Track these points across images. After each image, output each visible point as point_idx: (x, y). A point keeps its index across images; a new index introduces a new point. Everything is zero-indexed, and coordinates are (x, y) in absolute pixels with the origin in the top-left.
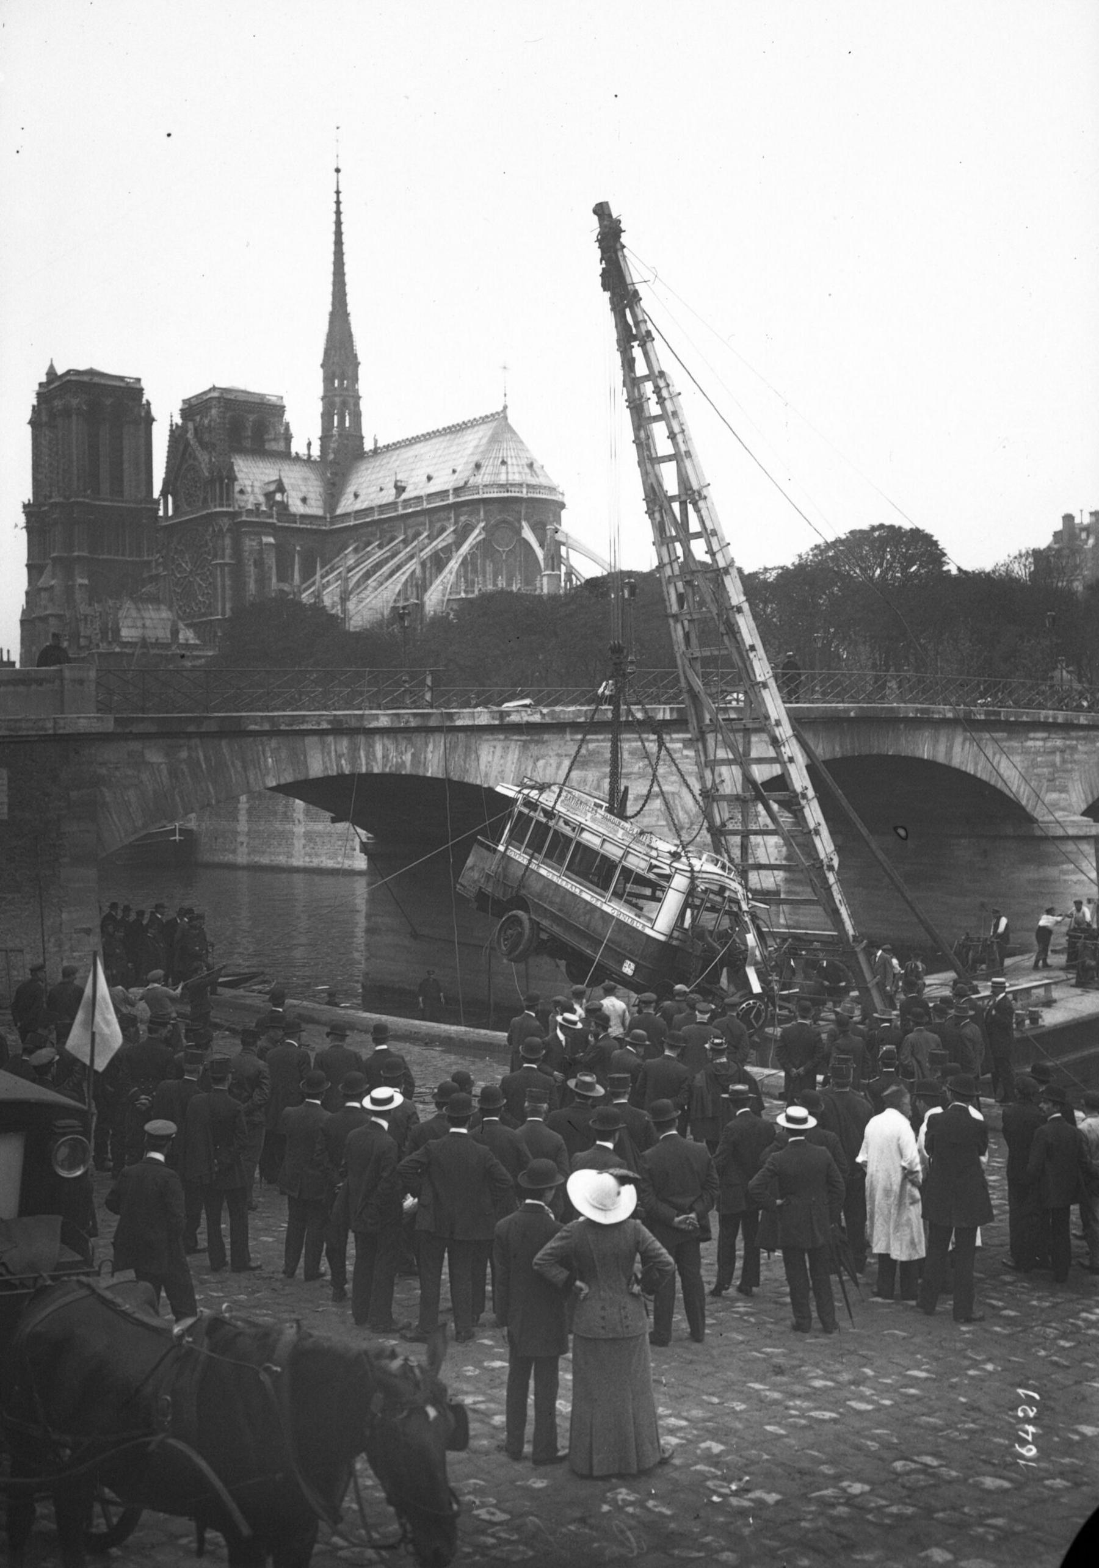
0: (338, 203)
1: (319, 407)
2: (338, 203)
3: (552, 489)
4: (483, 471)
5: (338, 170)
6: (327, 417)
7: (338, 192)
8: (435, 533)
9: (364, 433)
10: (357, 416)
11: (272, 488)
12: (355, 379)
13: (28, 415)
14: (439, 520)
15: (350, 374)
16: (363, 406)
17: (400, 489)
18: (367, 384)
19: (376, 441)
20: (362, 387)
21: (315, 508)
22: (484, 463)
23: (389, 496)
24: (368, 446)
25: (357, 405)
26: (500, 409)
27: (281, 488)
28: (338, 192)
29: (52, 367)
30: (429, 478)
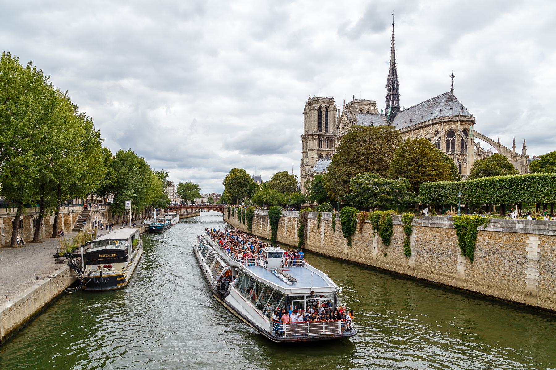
0: (393, 34)
1: (385, 99)
2: (393, 34)
3: (472, 117)
4: (443, 112)
5: (393, 24)
6: (388, 101)
8: (424, 135)
9: (400, 106)
10: (398, 101)
11: (369, 124)
12: (398, 89)
13: (303, 112)
14: (426, 130)
15: (396, 88)
16: (400, 98)
18: (402, 91)
20: (400, 92)
22: (443, 110)
23: (408, 124)
24: (401, 109)
25: (398, 97)
26: (450, 90)
28: (393, 31)
30: (422, 117)
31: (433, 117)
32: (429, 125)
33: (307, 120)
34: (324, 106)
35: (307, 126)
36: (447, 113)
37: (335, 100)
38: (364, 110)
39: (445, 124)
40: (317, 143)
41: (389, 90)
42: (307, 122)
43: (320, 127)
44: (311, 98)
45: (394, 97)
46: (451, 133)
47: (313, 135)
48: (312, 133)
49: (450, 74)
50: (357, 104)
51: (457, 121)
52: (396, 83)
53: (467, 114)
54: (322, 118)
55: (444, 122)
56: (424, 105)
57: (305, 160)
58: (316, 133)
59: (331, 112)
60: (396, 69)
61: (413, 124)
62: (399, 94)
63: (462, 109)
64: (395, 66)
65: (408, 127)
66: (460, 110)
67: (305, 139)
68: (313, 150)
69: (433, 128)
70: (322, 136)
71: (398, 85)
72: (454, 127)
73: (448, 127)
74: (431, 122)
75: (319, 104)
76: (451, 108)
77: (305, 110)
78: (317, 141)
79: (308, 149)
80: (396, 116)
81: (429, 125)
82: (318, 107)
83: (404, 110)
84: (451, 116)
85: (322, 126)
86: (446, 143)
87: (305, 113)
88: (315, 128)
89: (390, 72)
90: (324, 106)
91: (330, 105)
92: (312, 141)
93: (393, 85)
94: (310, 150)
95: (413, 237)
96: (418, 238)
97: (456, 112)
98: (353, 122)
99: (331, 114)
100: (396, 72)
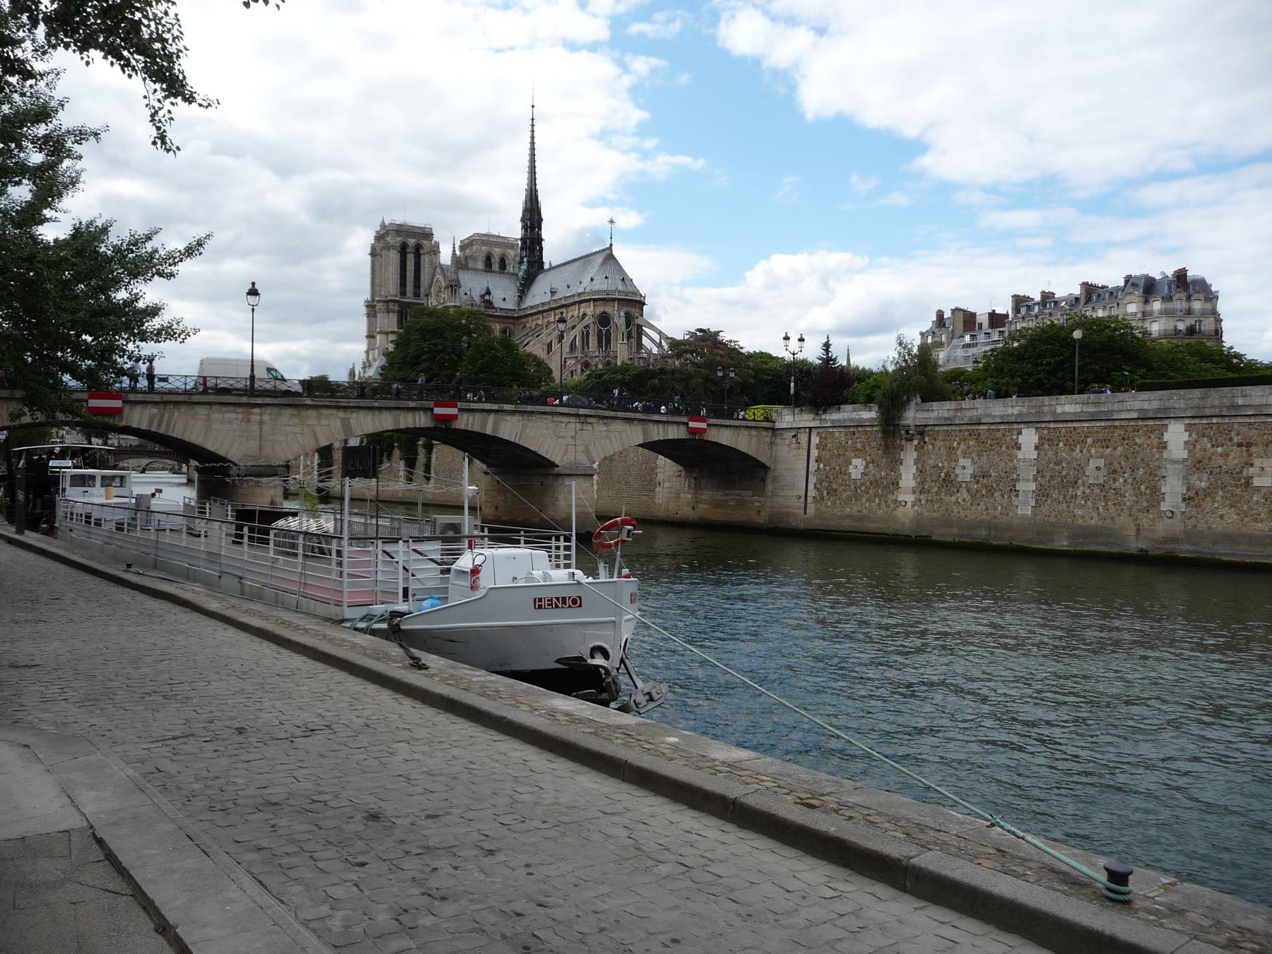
3: (636, 293)
5: (533, 107)
7: (533, 119)
12: (540, 229)
13: (369, 250)
14: (571, 311)
17: (553, 293)
19: (550, 264)
20: (545, 233)
21: (510, 304)
22: (595, 278)
23: (547, 298)
24: (546, 266)
26: (608, 246)
27: (488, 292)
28: (533, 119)
29: (383, 221)
30: (568, 287)
31: (581, 290)
32: (574, 304)
33: (377, 268)
34: (412, 242)
35: (377, 281)
36: (600, 285)
37: (434, 232)
38: (495, 255)
39: (596, 303)
40: (396, 320)
41: (525, 228)
42: (377, 273)
43: (403, 284)
44: (387, 224)
45: (532, 243)
46: (604, 320)
47: (387, 302)
48: (387, 297)
49: (608, 219)
50: (480, 242)
51: (614, 300)
52: (536, 217)
53: (630, 289)
54: (408, 268)
55: (595, 300)
56: (576, 264)
57: (371, 353)
58: (393, 298)
59: (427, 256)
60: (536, 191)
61: (556, 297)
62: (543, 237)
63: (623, 279)
64: (535, 185)
65: (549, 303)
66: (620, 282)
67: (371, 308)
68: (387, 333)
69: (579, 309)
70: (409, 305)
71: (540, 220)
72: (608, 309)
73: (600, 310)
74: (576, 299)
75: (400, 239)
76: (606, 277)
77: (373, 248)
78: (396, 314)
79: (378, 330)
80: (535, 277)
81: (574, 304)
82: (399, 244)
83: (552, 268)
84: (604, 291)
85: (408, 284)
86: (598, 335)
87: (374, 254)
88: (392, 287)
89: (526, 196)
90: (412, 242)
91: (425, 242)
92: (386, 315)
93: (531, 219)
94: (380, 332)
95: (434, 456)
96: (437, 458)
97: (615, 285)
98: (452, 286)
99: (425, 260)
100: (537, 197)
